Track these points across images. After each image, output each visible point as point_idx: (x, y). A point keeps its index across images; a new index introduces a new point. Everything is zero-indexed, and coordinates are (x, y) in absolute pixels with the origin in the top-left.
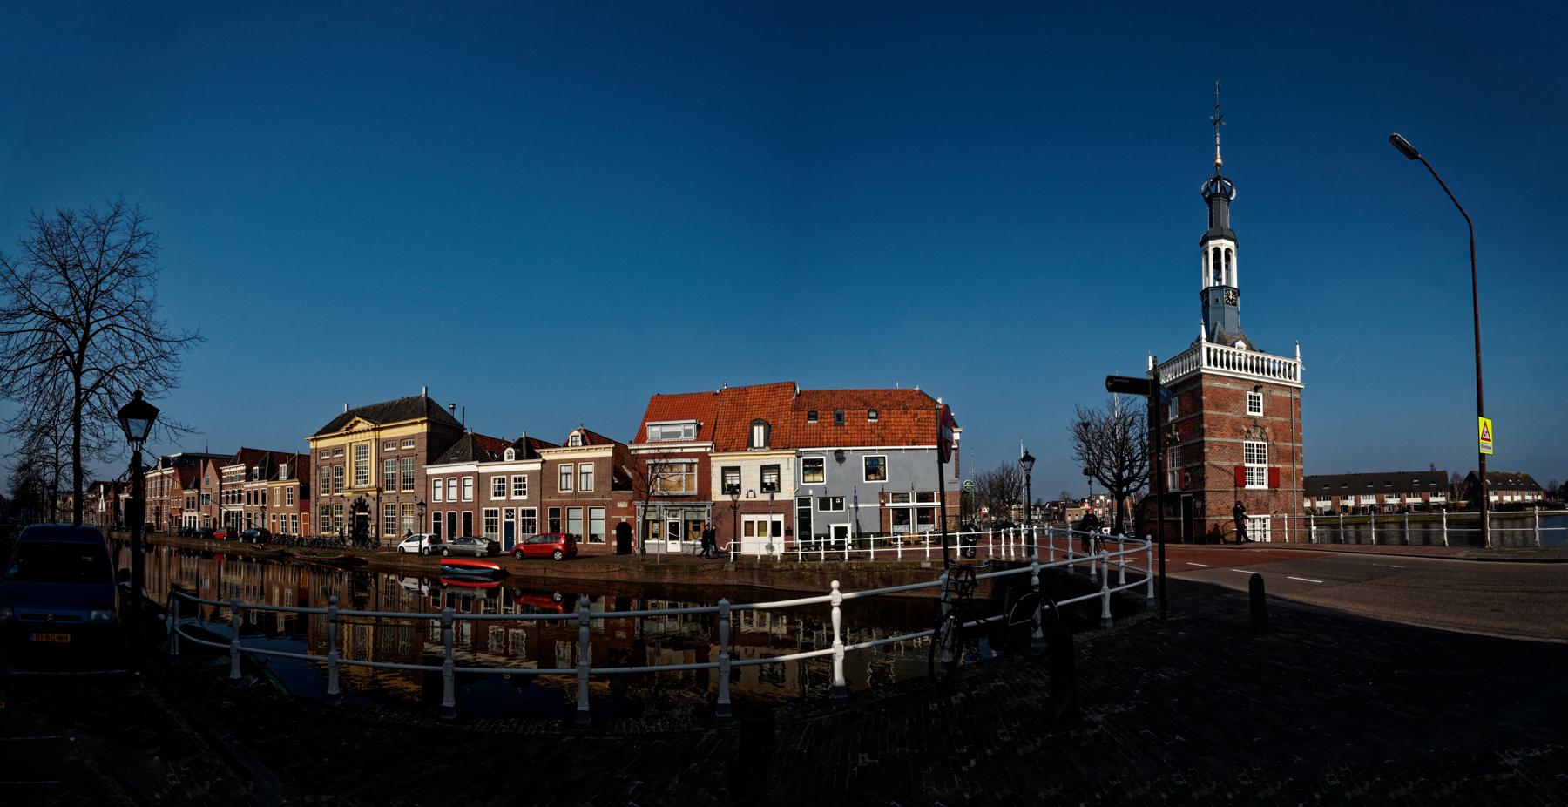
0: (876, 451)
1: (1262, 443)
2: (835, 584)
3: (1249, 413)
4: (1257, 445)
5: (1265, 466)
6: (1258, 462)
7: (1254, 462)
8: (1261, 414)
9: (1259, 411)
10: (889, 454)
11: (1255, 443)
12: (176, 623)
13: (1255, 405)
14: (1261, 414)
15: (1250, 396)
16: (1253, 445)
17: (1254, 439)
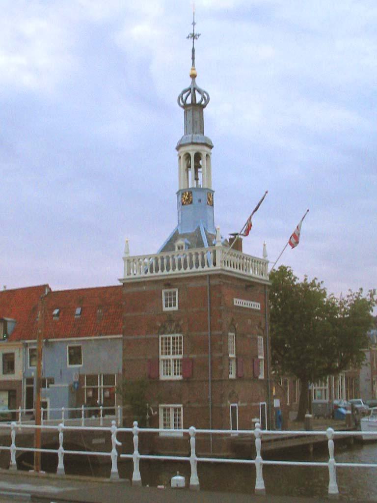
0: (75, 341)
1: (178, 335)
2: (136, 423)
3: (165, 309)
4: (173, 338)
5: (171, 357)
6: (173, 353)
7: (169, 353)
8: (176, 308)
9: (166, 306)
10: (88, 343)
11: (171, 336)
12: (374, 379)
13: (170, 299)
14: (176, 308)
15: (166, 294)
16: (169, 339)
17: (169, 333)
